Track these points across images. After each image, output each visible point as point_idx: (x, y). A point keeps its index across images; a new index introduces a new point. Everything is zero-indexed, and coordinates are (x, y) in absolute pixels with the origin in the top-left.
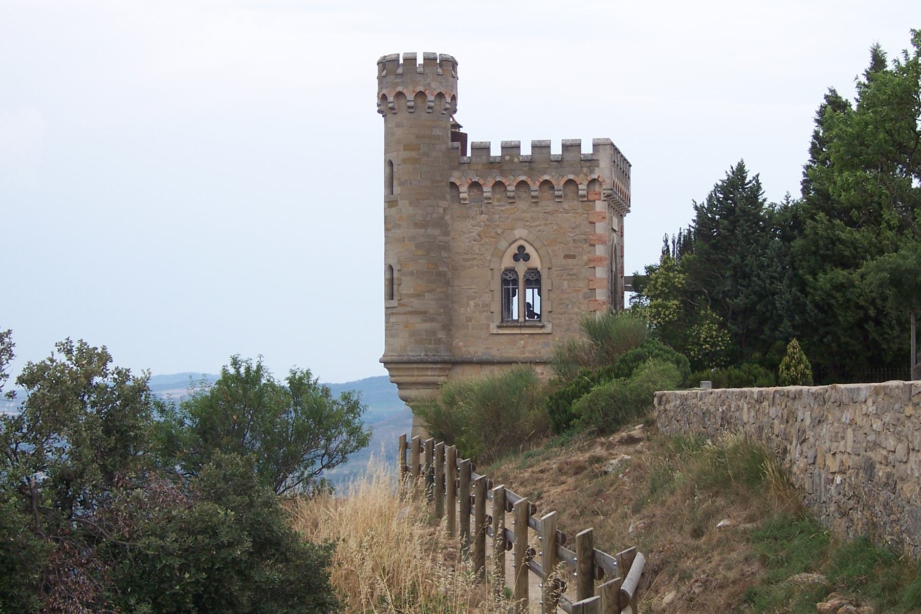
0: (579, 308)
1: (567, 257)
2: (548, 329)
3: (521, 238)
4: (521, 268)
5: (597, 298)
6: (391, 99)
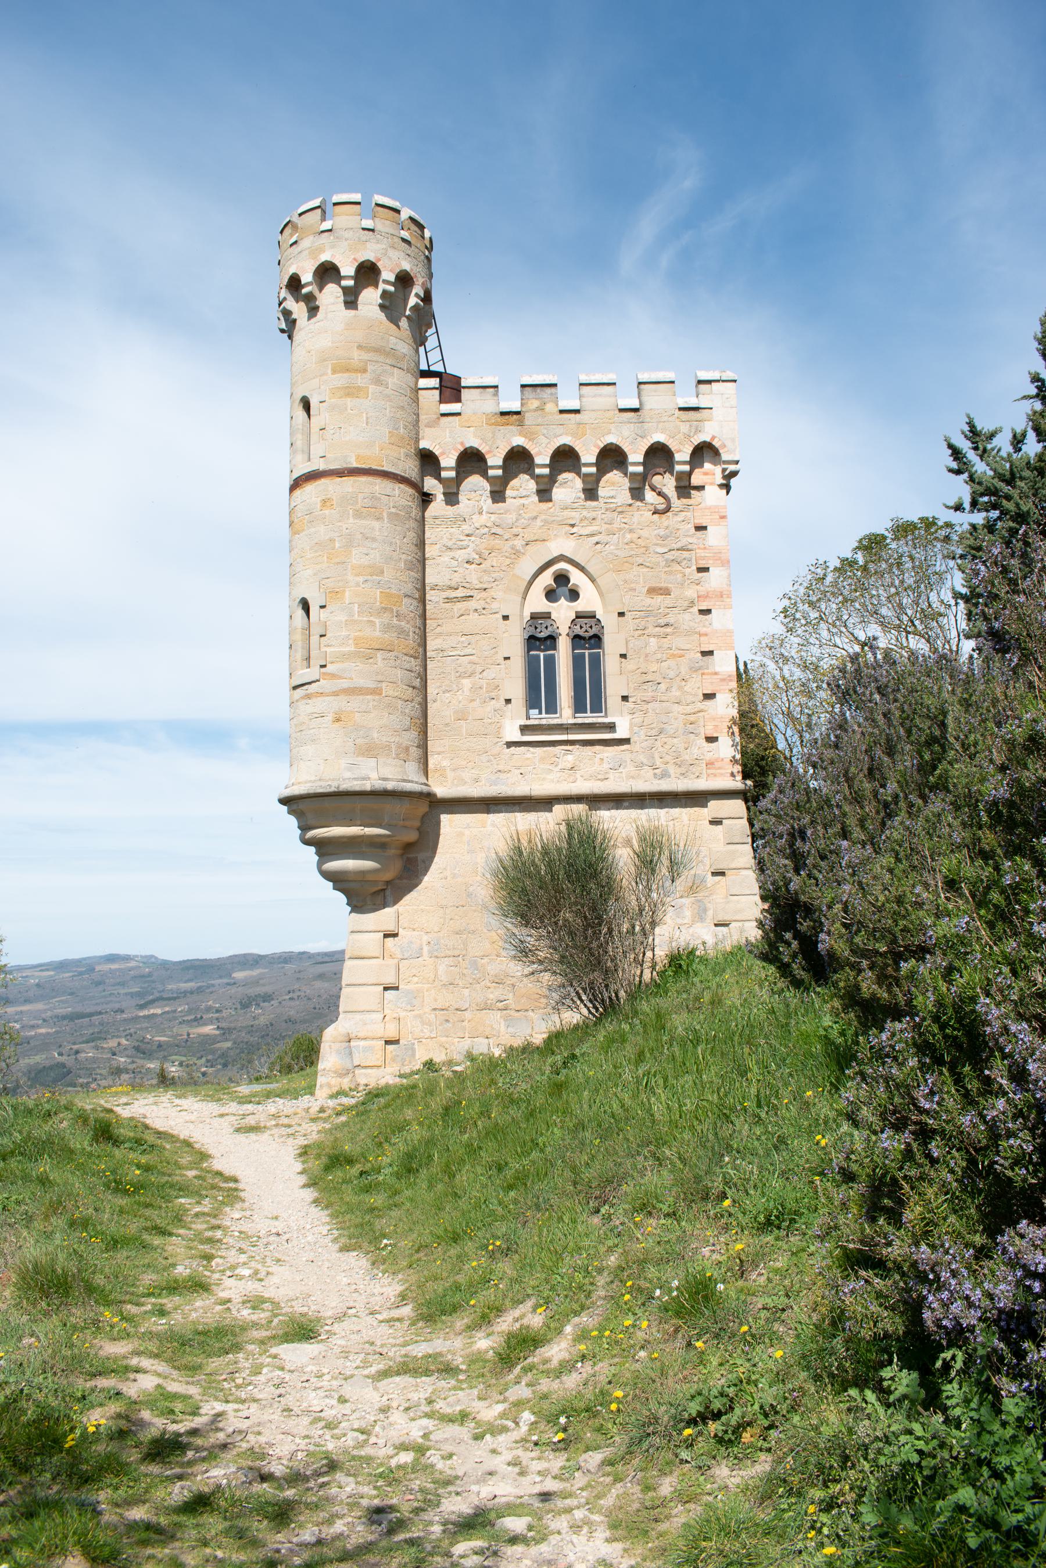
0: (680, 688)
1: (652, 591)
2: (620, 733)
3: (562, 558)
4: (563, 613)
5: (718, 669)
6: (307, 277)
